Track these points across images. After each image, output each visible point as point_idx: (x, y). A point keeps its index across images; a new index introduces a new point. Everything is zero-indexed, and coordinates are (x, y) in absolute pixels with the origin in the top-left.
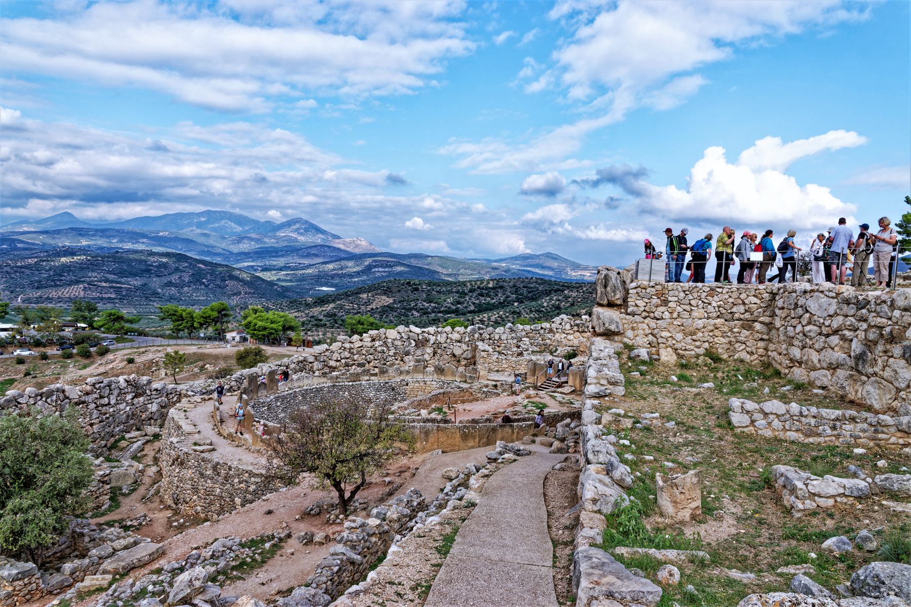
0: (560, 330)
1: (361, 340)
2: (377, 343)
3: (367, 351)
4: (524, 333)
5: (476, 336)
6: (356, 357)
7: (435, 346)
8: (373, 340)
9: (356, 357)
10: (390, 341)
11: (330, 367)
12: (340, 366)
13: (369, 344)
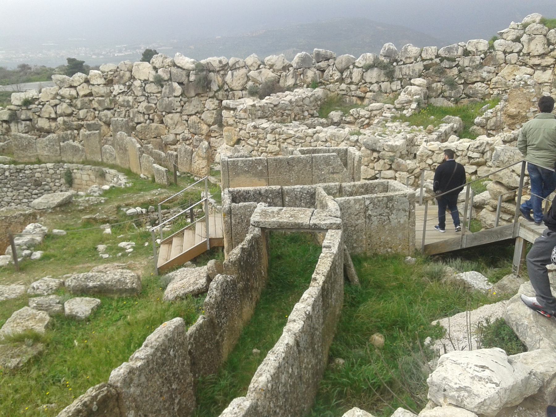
0: (513, 58)
1: (87, 81)
2: (117, 88)
3: (99, 102)
4: (419, 66)
5: (310, 74)
6: (82, 113)
7: (220, 94)
8: (109, 83)
9: (82, 113)
10: (137, 83)
11: (41, 130)
12: (57, 128)
13: (103, 90)
